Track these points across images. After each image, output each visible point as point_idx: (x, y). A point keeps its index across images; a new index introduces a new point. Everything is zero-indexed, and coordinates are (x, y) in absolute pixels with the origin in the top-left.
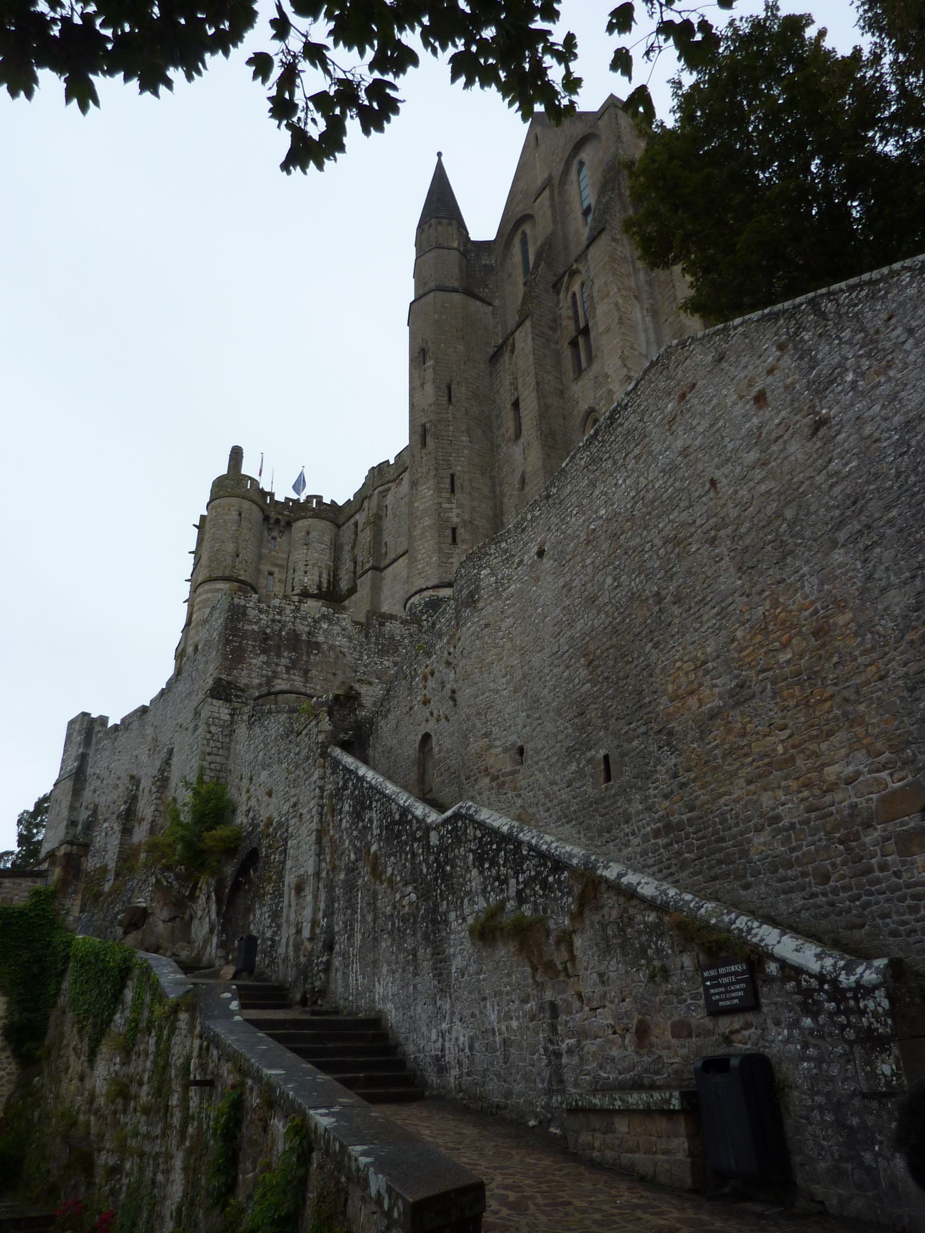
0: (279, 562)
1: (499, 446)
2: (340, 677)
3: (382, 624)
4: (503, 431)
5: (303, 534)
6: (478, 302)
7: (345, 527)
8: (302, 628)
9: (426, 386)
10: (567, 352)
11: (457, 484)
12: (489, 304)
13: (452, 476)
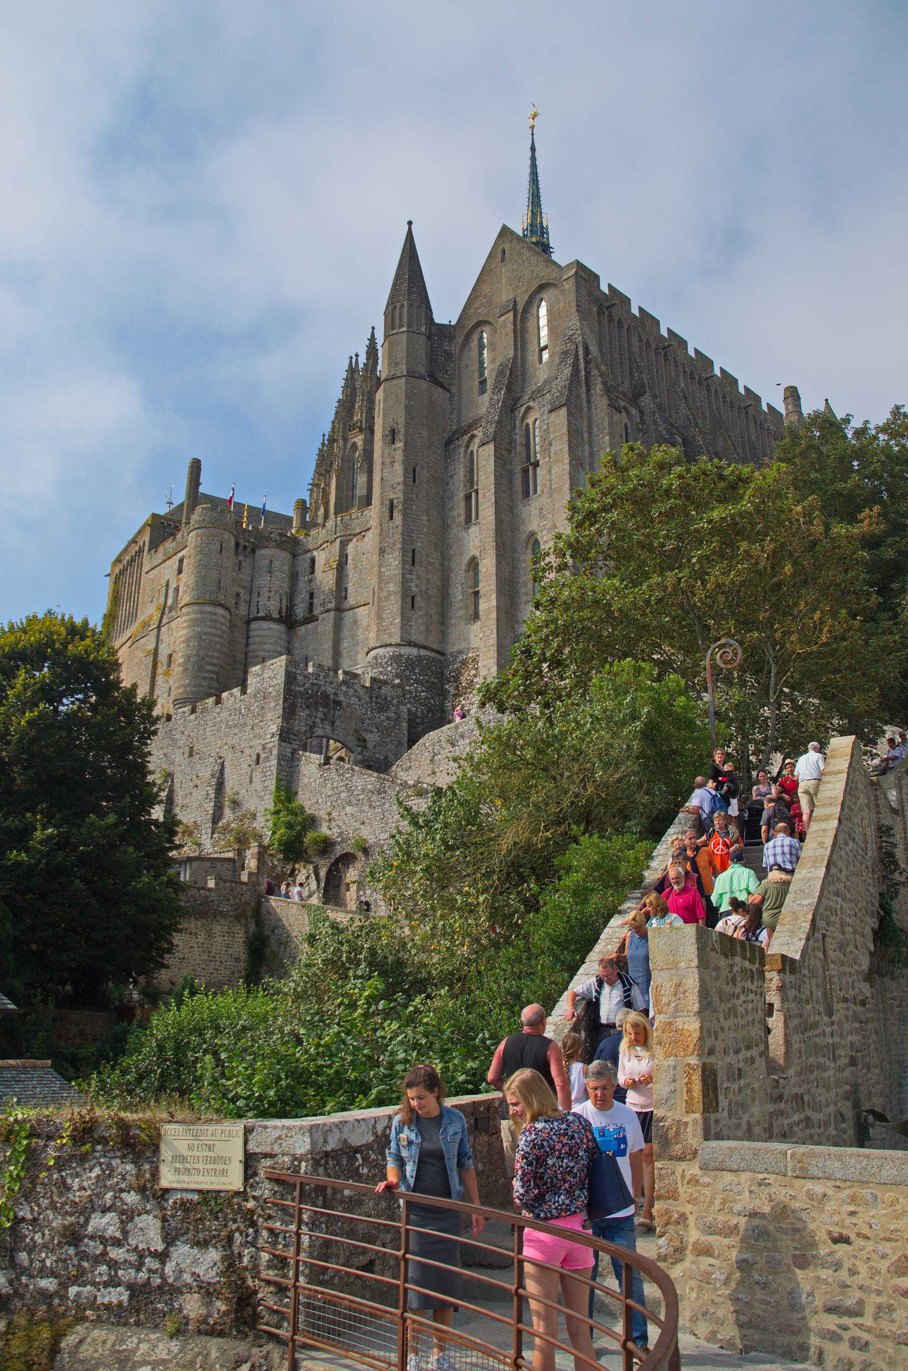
0: (245, 584)
1: (450, 526)
3: (380, 688)
4: (455, 514)
5: (267, 562)
6: (439, 389)
7: (300, 558)
8: (330, 690)
9: (396, 465)
10: (518, 476)
11: (417, 557)
12: (448, 391)
13: (414, 551)
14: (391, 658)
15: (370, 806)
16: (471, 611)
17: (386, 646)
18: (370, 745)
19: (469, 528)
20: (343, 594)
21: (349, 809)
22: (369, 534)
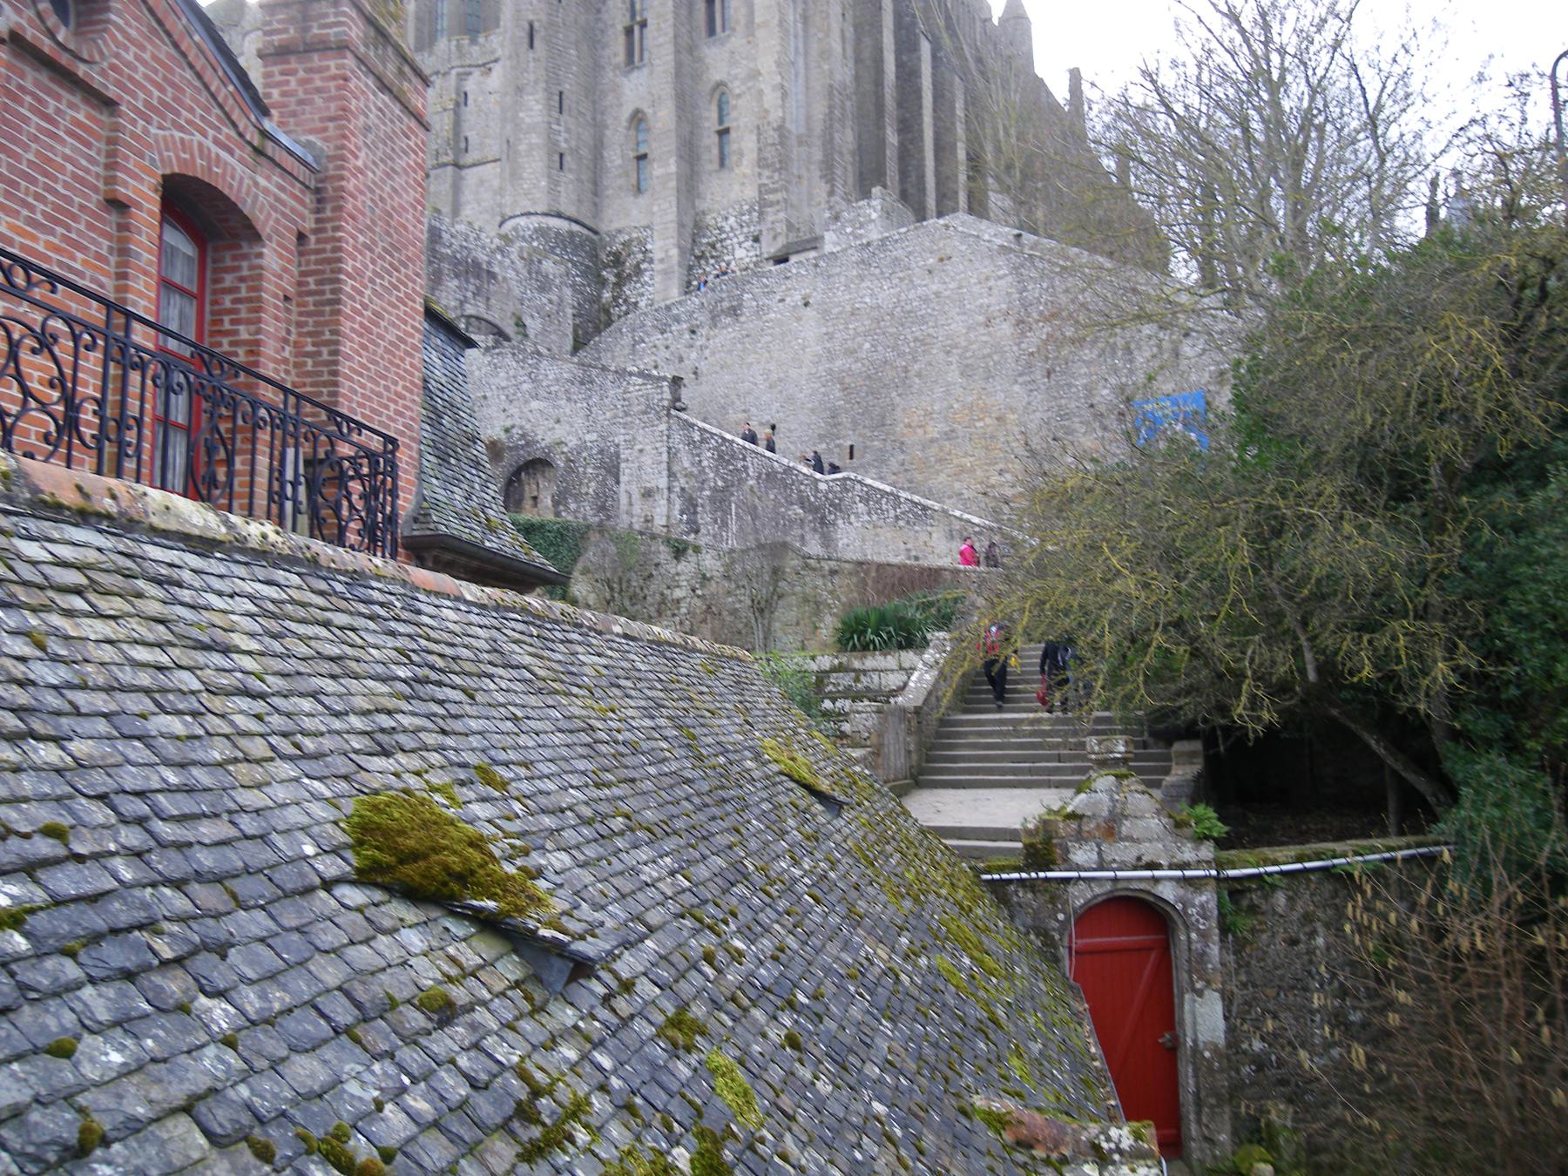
2: (512, 309)
3: (540, 262)
11: (566, 103)
13: (561, 93)
14: (536, 230)
15: (569, 399)
16: (634, 181)
17: (528, 214)
18: (531, 333)
19: (630, 72)
20: (463, 145)
21: (535, 404)
22: (497, 69)
